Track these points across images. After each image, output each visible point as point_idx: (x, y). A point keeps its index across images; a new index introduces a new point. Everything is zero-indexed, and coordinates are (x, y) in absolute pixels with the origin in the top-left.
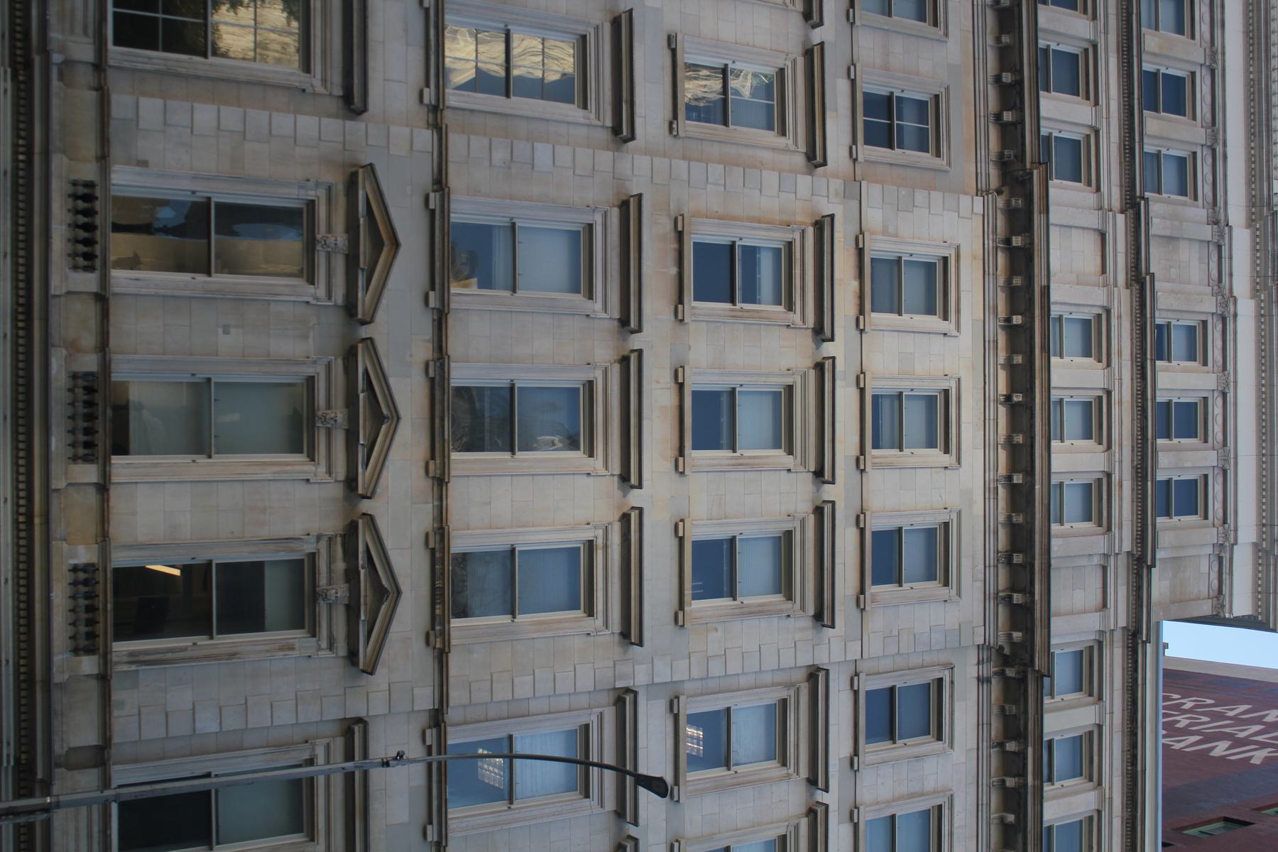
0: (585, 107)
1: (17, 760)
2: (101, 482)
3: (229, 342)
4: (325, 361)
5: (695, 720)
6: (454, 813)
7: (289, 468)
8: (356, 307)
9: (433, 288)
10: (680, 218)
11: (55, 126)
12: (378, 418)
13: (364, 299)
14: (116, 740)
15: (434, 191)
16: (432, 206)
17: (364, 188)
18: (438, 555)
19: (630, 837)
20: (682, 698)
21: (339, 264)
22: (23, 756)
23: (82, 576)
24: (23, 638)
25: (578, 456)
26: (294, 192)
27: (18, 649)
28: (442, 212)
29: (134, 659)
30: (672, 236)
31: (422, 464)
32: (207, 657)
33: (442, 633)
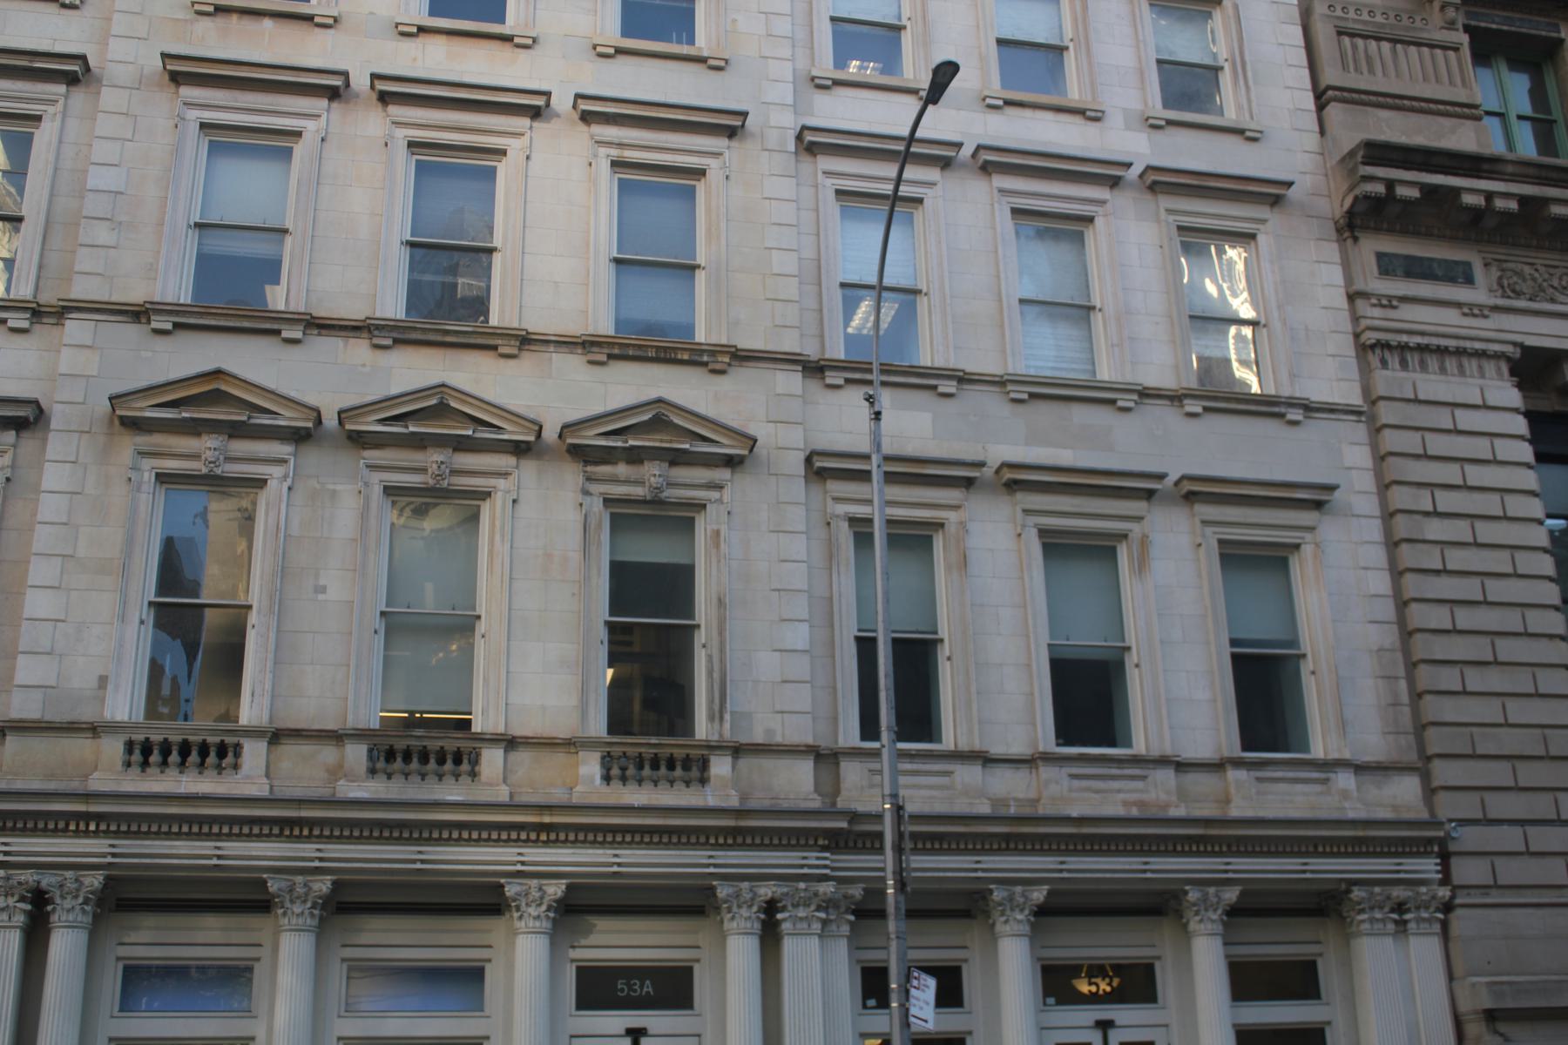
0: (38, 118)
1: (824, 849)
2: (503, 744)
3: (337, 588)
4: (366, 472)
5: (840, 63)
6: (925, 359)
7: (498, 523)
8: (298, 429)
9: (278, 332)
10: (197, 7)
11: (52, 786)
12: (441, 411)
13: (288, 418)
14: (810, 741)
15: (149, 322)
16: (169, 326)
17: (141, 409)
18: (616, 351)
19: (974, 156)
20: (815, 73)
21: (241, 447)
22: (820, 842)
23: (615, 771)
24: (684, 840)
25: (503, 169)
26: (144, 498)
27: (697, 845)
28: (177, 313)
29: (717, 715)
30: (220, 20)
31: (502, 361)
32: (721, 632)
33: (713, 353)
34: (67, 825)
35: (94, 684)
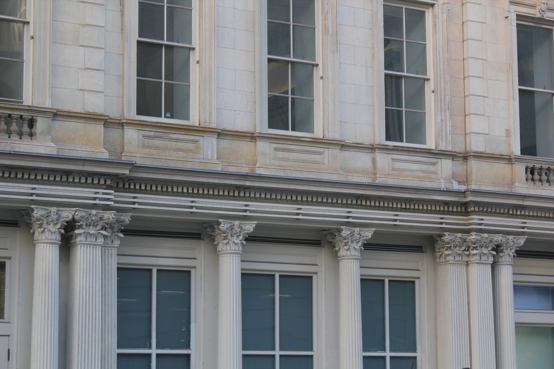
34: (509, 211)
35: (504, 134)
